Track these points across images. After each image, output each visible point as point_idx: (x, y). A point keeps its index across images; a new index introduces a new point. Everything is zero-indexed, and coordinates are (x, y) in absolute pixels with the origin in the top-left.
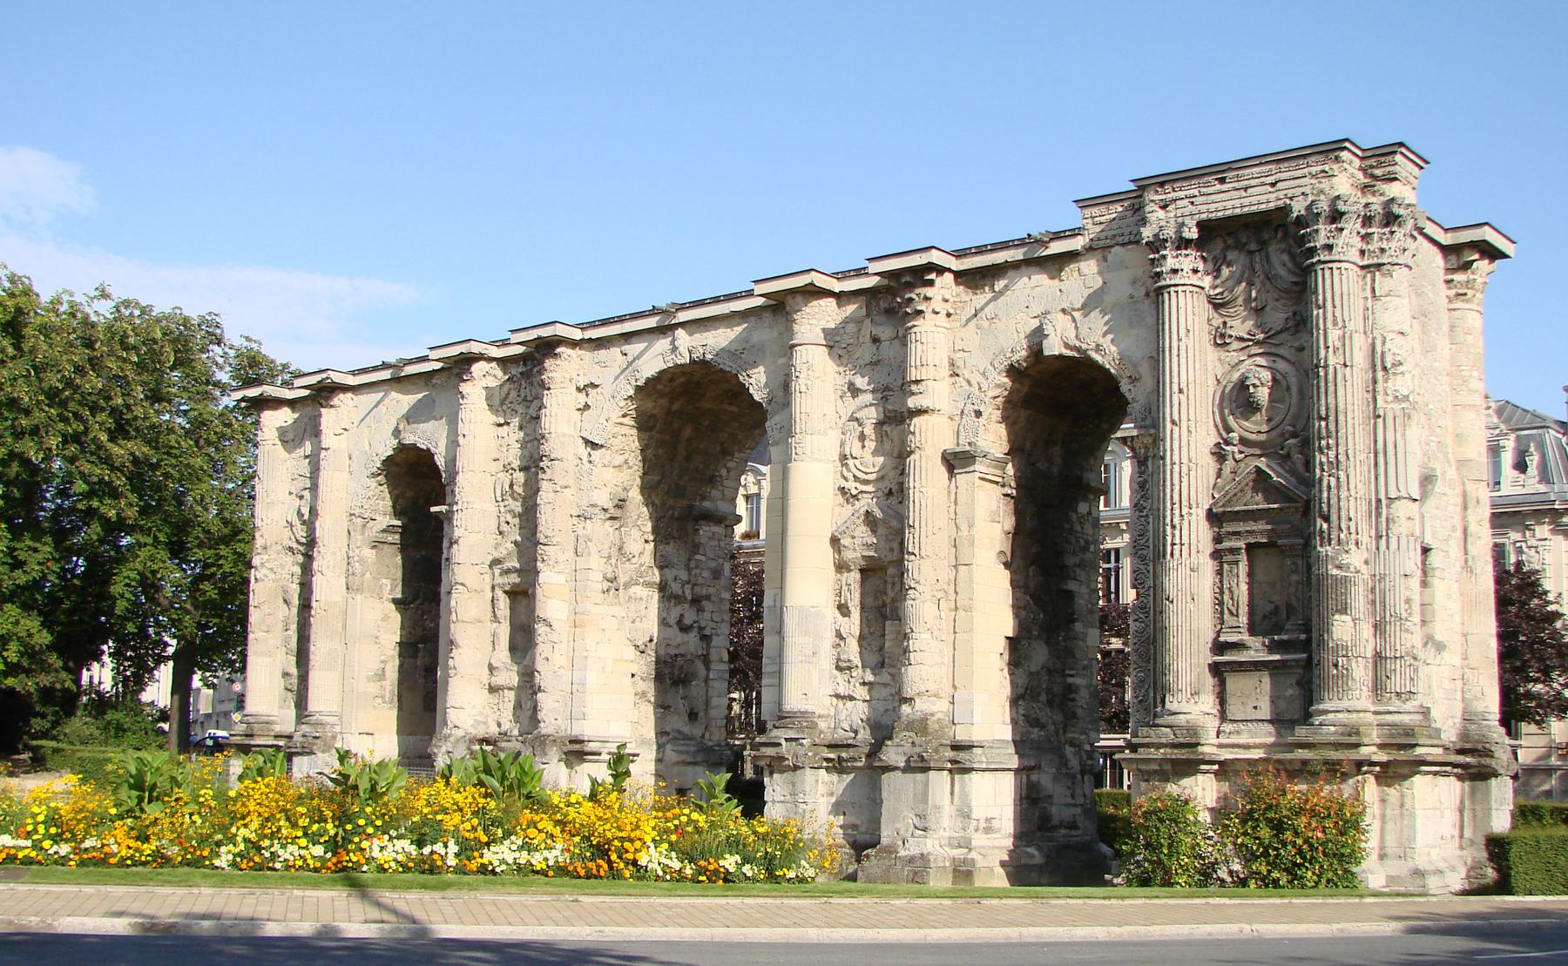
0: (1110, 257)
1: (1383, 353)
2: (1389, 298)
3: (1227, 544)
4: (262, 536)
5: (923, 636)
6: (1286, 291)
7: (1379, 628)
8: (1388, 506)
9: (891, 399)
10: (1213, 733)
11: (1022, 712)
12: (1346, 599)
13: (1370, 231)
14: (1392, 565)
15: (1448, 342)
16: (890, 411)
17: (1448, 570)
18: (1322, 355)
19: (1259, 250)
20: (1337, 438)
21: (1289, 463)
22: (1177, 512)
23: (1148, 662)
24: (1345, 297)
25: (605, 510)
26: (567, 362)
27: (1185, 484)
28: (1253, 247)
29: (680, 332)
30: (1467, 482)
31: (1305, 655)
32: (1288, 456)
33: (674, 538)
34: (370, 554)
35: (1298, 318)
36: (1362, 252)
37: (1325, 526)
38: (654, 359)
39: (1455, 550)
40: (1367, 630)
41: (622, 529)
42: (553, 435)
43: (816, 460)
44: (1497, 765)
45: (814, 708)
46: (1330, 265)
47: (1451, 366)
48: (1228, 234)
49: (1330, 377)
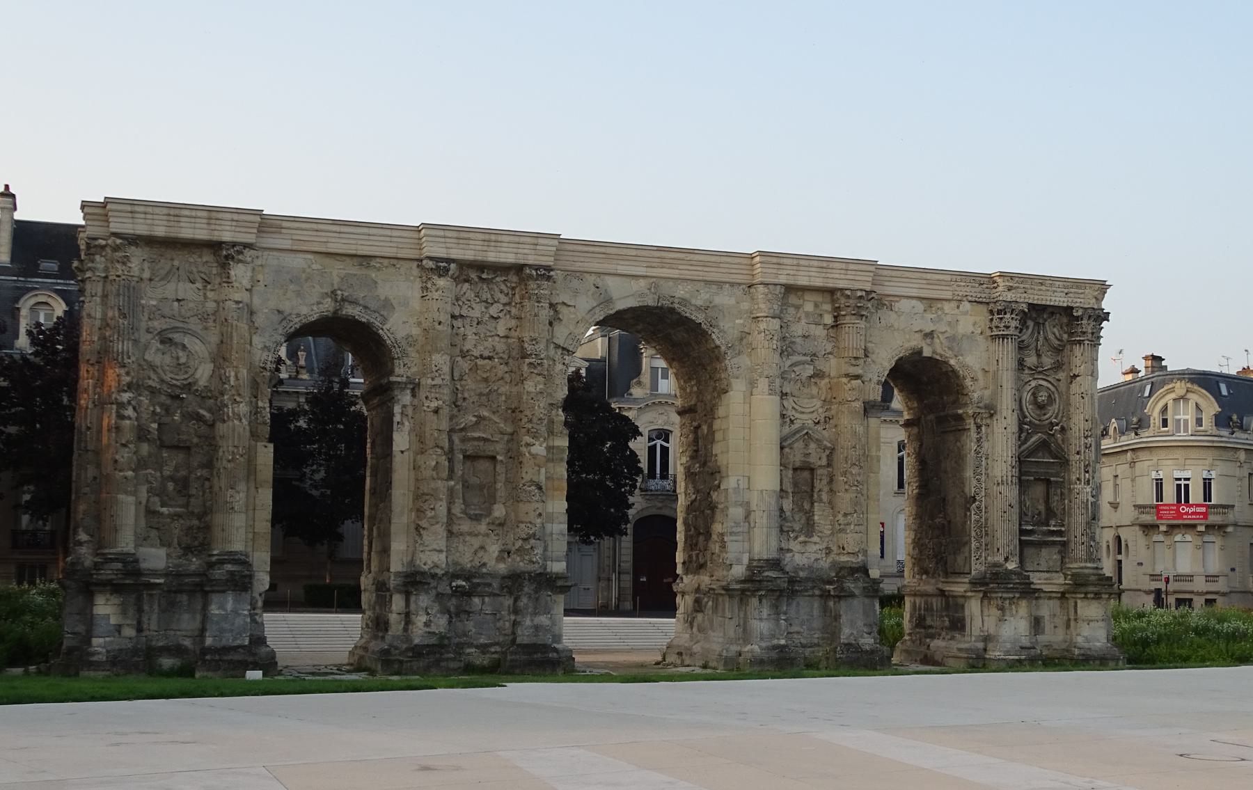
3: (1023, 478)
4: (128, 374)
6: (1055, 348)
9: (817, 362)
16: (817, 370)
23: (982, 537)
28: (1041, 321)
37: (1087, 475)
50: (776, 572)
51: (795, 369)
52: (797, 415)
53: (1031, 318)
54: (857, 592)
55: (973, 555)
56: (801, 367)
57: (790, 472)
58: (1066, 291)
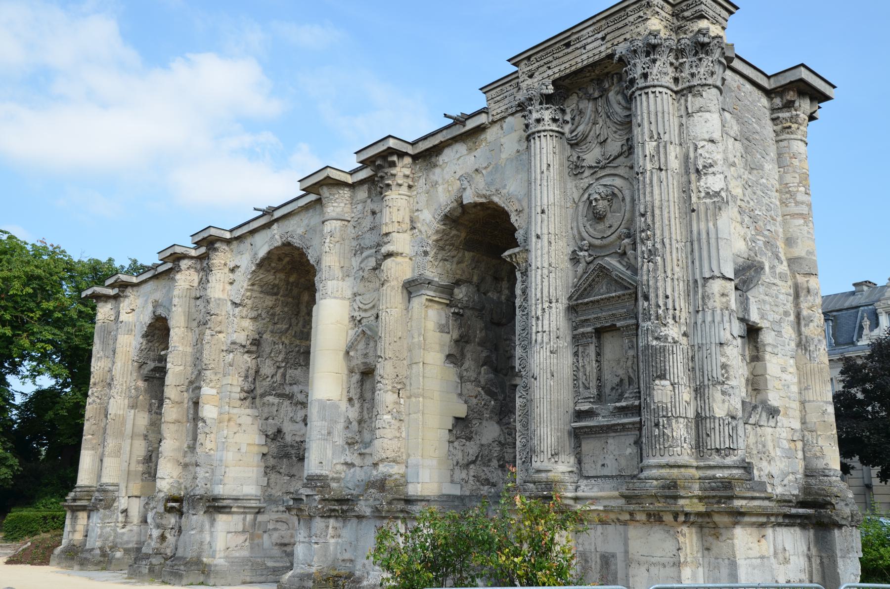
0: (505, 126)
1: (696, 157)
2: (699, 114)
5: (385, 417)
7: (699, 391)
8: (704, 286)
10: (571, 487)
11: (472, 474)
12: (665, 366)
13: (681, 61)
14: (708, 335)
15: (776, 167)
17: (780, 347)
18: (641, 163)
19: (601, 96)
20: (654, 229)
21: (626, 259)
22: (540, 306)
24: (660, 115)
25: (244, 346)
26: (222, 254)
27: (546, 283)
28: (596, 95)
29: (275, 226)
30: (798, 276)
31: (638, 419)
32: (625, 253)
33: (300, 365)
34: (141, 384)
35: (630, 143)
36: (676, 80)
37: (646, 304)
38: (263, 244)
39: (788, 332)
40: (686, 395)
41: (259, 359)
42: (213, 300)
43: (335, 298)
44: (837, 515)
45: (327, 472)
46: (646, 91)
47: (780, 184)
48: (580, 90)
49: (648, 181)
50: (308, 490)
51: (362, 265)
52: (363, 315)
53: (590, 98)
54: (368, 511)
55: (518, 457)
56: (366, 261)
57: (356, 377)
58: (600, 35)
